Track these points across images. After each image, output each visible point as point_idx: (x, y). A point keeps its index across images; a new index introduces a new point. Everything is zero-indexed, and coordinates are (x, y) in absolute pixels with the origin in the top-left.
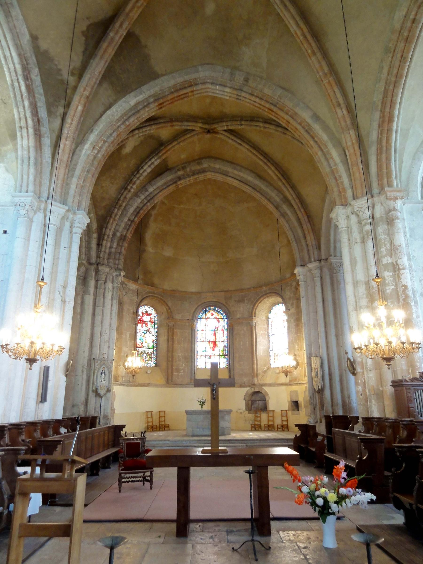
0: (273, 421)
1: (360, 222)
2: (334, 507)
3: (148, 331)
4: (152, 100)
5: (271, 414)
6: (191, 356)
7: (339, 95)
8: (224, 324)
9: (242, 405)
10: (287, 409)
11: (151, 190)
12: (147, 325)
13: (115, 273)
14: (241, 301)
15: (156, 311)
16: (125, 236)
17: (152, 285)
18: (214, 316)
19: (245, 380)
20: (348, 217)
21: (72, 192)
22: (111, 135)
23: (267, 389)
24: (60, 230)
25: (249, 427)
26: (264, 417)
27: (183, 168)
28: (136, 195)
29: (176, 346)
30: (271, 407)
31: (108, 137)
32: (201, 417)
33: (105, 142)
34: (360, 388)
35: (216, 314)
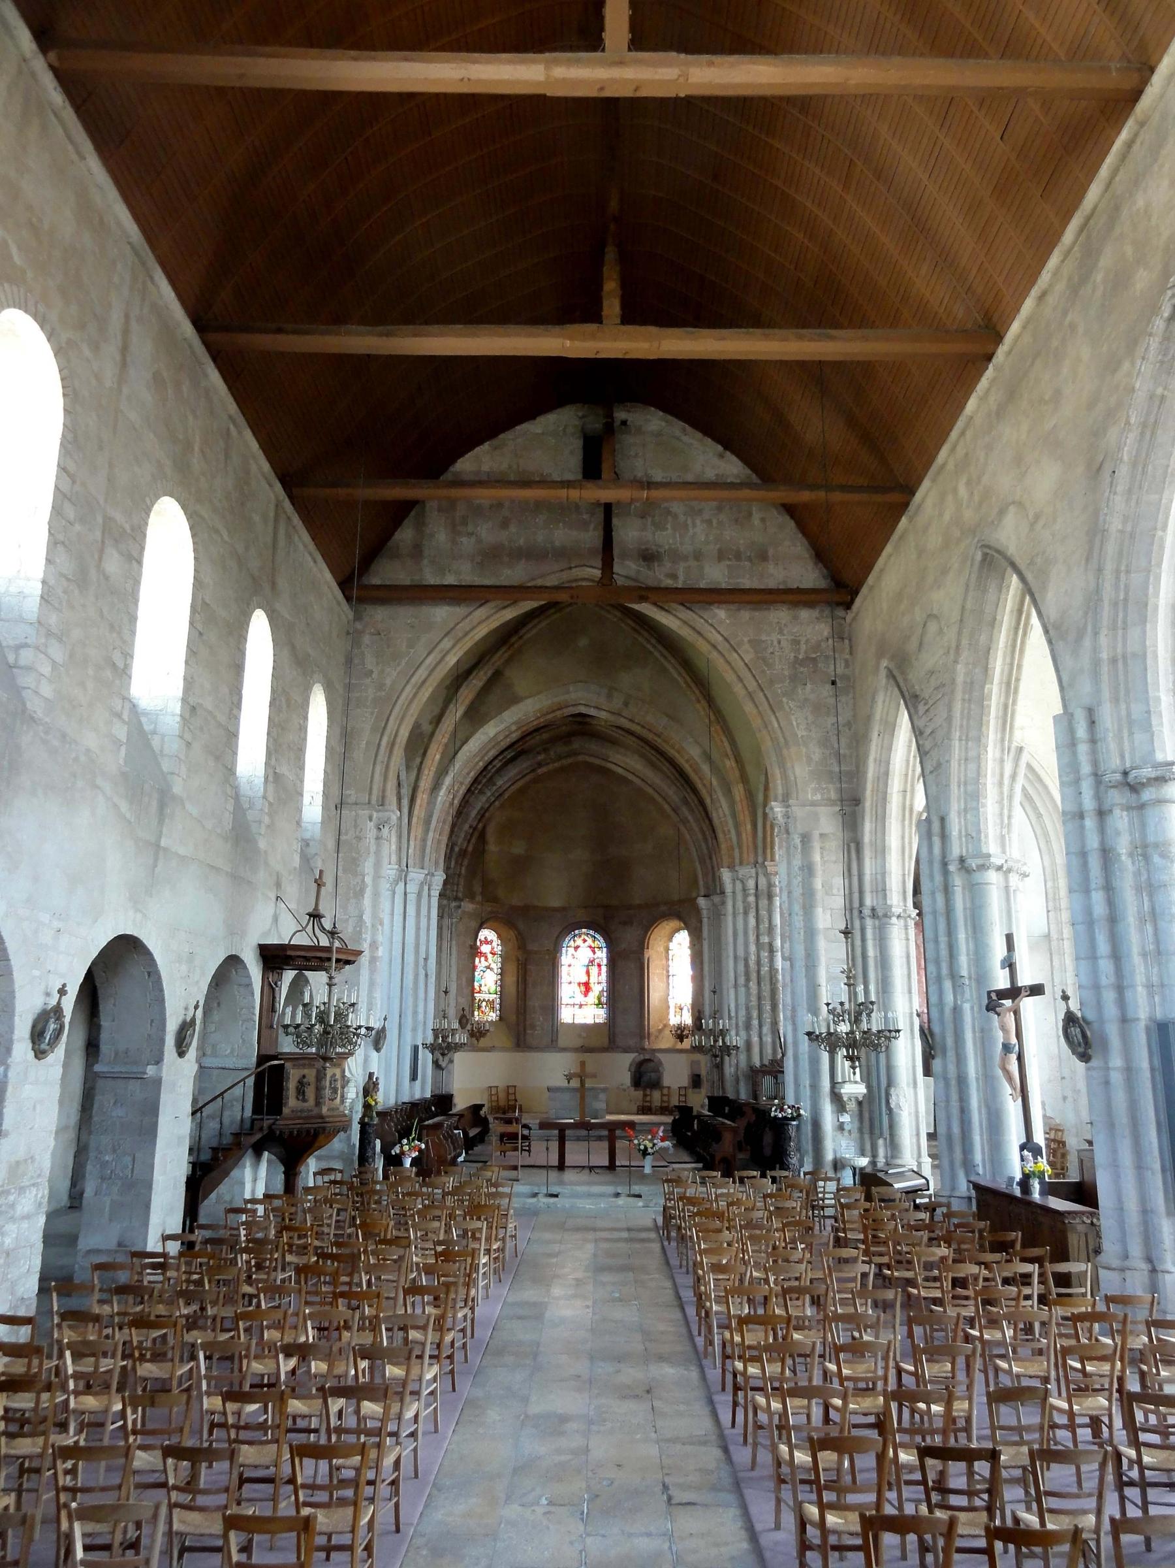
0: (668, 1102)
1: (744, 890)
2: (650, 1150)
3: (488, 967)
4: (514, 728)
5: (665, 1091)
6: (553, 1008)
7: (726, 744)
8: (602, 956)
9: (626, 1079)
10: (686, 1085)
11: (500, 783)
12: (486, 960)
13: (454, 904)
14: (627, 923)
15: (499, 937)
16: (465, 851)
17: (495, 900)
18: (587, 944)
19: (632, 1042)
20: (734, 881)
21: (428, 850)
22: (468, 774)
23: (659, 1055)
24: (419, 895)
25: (635, 1109)
26: (656, 1095)
27: (545, 750)
28: (481, 792)
29: (530, 990)
30: (666, 1082)
31: (465, 778)
32: (566, 1096)
33: (461, 784)
34: (732, 1070)
35: (590, 941)
